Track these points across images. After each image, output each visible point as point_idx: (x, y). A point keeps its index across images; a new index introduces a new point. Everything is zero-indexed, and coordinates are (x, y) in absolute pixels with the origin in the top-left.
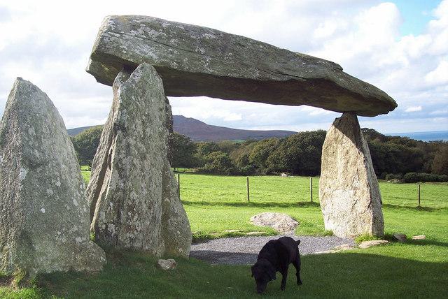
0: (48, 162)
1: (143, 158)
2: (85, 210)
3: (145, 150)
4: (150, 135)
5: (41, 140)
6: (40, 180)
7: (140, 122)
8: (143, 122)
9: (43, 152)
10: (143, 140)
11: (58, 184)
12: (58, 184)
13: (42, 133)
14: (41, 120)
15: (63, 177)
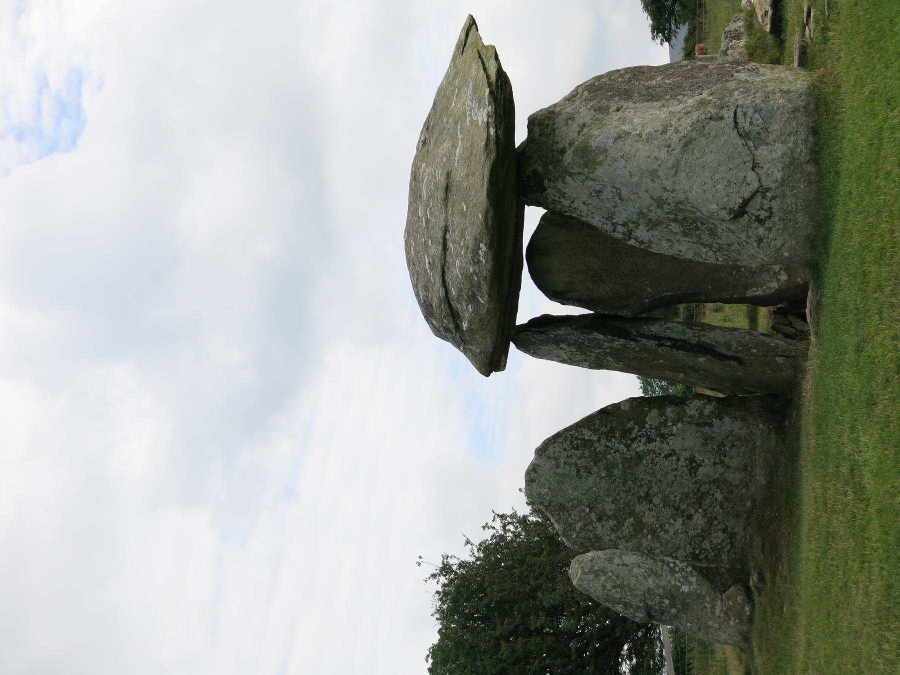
0: (647, 603)
1: (639, 526)
2: (693, 579)
3: (631, 520)
4: (613, 502)
5: (627, 603)
6: (662, 614)
7: (599, 525)
8: (600, 519)
9: (638, 607)
10: (620, 524)
11: (667, 602)
12: (667, 602)
13: (620, 599)
14: (607, 595)
15: (661, 591)
